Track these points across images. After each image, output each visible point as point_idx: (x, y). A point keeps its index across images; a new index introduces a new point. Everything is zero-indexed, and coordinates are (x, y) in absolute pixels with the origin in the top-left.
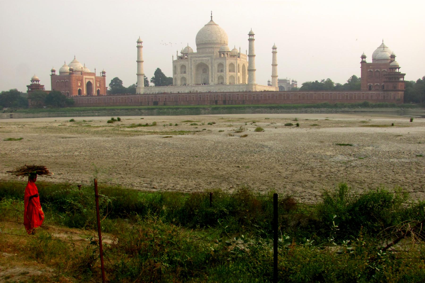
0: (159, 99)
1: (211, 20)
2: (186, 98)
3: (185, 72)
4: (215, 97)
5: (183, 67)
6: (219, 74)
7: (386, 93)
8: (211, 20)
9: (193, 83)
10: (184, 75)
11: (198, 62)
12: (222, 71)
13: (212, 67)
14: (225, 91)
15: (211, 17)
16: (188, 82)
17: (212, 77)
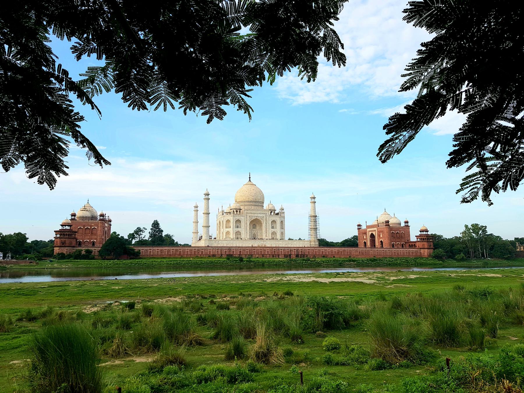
0: (233, 251)
1: (250, 181)
2: (261, 251)
3: (238, 227)
4: (288, 252)
5: (238, 221)
6: (273, 230)
7: (422, 250)
8: (250, 181)
9: (248, 237)
10: (239, 229)
11: (253, 218)
12: (273, 228)
13: (266, 223)
14: (292, 246)
15: (250, 178)
16: (243, 236)
17: (266, 233)
